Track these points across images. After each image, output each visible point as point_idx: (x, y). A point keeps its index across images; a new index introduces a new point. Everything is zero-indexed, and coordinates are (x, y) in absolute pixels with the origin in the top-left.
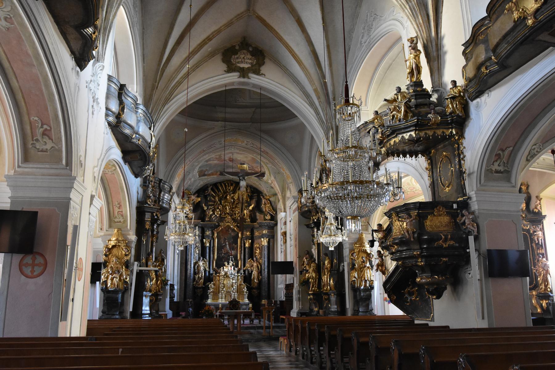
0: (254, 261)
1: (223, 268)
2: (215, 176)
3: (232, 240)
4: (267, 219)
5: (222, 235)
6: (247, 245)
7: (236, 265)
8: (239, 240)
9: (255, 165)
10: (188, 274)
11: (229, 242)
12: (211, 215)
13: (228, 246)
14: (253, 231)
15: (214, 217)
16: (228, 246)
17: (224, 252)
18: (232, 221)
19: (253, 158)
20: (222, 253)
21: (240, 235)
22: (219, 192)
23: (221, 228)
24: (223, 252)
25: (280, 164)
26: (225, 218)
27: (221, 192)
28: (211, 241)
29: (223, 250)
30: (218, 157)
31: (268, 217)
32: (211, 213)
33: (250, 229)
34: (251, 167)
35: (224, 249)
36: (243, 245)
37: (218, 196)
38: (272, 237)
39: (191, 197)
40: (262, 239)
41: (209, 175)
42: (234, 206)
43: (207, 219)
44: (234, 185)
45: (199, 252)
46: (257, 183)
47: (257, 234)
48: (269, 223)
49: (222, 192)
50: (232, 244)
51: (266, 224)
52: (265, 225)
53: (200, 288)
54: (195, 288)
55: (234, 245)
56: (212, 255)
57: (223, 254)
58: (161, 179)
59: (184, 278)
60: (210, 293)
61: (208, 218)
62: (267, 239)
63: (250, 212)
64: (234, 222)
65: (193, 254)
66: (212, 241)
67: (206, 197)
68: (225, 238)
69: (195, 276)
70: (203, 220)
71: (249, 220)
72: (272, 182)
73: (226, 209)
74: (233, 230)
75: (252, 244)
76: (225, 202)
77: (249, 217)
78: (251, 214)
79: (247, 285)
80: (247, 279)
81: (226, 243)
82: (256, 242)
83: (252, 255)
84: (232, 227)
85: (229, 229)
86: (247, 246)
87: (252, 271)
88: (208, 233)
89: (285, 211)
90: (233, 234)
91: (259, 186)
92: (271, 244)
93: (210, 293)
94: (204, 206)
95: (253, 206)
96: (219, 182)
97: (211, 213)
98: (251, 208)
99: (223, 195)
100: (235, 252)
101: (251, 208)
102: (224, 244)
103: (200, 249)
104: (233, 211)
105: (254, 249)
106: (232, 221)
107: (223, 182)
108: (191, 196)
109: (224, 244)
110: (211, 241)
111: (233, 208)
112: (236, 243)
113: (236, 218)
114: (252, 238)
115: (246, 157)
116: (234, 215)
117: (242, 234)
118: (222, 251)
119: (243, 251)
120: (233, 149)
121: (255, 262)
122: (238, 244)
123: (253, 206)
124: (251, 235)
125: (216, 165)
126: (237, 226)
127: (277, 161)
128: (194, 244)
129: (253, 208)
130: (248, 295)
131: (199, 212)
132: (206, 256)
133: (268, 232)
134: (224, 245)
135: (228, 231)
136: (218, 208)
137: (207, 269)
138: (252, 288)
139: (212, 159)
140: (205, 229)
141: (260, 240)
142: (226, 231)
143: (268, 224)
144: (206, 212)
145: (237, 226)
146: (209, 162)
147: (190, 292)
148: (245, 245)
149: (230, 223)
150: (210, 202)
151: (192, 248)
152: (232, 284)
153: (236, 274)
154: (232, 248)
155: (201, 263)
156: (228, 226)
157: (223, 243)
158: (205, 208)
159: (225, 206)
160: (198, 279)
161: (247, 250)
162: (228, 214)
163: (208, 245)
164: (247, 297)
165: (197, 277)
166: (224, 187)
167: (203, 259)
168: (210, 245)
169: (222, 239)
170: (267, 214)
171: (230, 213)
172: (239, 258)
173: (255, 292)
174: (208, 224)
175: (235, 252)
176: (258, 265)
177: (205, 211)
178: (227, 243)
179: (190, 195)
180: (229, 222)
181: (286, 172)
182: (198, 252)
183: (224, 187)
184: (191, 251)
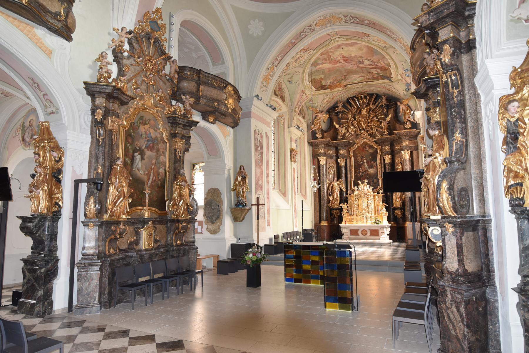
2: (340, 89)
4: (407, 129)
5: (359, 153)
9: (375, 58)
10: (322, 195)
11: (366, 160)
12: (345, 134)
13: (365, 164)
14: (394, 145)
15: (348, 136)
16: (365, 164)
17: (363, 170)
18: (369, 137)
19: (368, 46)
20: (360, 172)
21: (379, 152)
22: (351, 107)
23: (357, 146)
24: (361, 171)
25: (394, 34)
26: (360, 134)
27: (354, 107)
28: (346, 160)
29: (361, 169)
30: (325, 57)
31: (408, 126)
32: (344, 131)
33: (389, 143)
34: (372, 63)
35: (362, 168)
36: (382, 161)
37: (352, 112)
38: (414, 150)
39: (318, 115)
40: (402, 152)
41: (331, 87)
42: (369, 120)
43: (339, 138)
44: (368, 98)
45: (334, 172)
46: (391, 88)
47: (397, 147)
48: (410, 132)
49: (356, 107)
50: (371, 162)
51: (405, 134)
52: (404, 136)
53: (336, 209)
54: (330, 210)
55: (373, 162)
56: (349, 176)
57: (361, 173)
58: (199, 69)
59: (318, 199)
61: (341, 136)
62: (409, 151)
64: (370, 137)
65: (325, 175)
66: (348, 161)
67: (337, 114)
68: (362, 156)
69: (330, 197)
70: (335, 138)
71: (386, 133)
72: (402, 77)
73: (361, 124)
74: (371, 147)
75: (393, 159)
76: (359, 117)
77: (387, 129)
78: (388, 126)
79: (385, 206)
82: (397, 156)
84: (368, 143)
85: (366, 145)
88: (341, 152)
90: (371, 151)
91: (394, 90)
92: (415, 157)
94: (335, 125)
95: (390, 116)
96: (351, 98)
97: (344, 131)
98: (388, 119)
99: (356, 111)
100: (374, 170)
101: (388, 119)
102: (361, 163)
103: (335, 169)
104: (368, 126)
105: (396, 165)
106: (369, 137)
107: (355, 96)
108: (318, 114)
109: (361, 163)
110: (346, 160)
111: (369, 123)
113: (373, 133)
114: (393, 153)
115: (360, 49)
117: (381, 150)
119: (383, 169)
120: (337, 39)
122: (377, 161)
123: (390, 116)
124: (390, 149)
125: (329, 70)
126: (374, 141)
127: (388, 32)
129: (391, 119)
131: (331, 132)
132: (342, 176)
133: (409, 143)
134: (362, 164)
135: (365, 148)
136: (353, 125)
137: (344, 190)
138: (395, 209)
139: (319, 62)
140: (339, 148)
142: (363, 148)
146: (319, 67)
147: (324, 215)
149: (367, 139)
150: (342, 119)
151: (323, 168)
153: (372, 193)
154: (370, 167)
155: (335, 184)
156: (365, 142)
157: (360, 161)
158: (337, 126)
159: (360, 121)
160: (333, 200)
161: (387, 167)
162: (364, 129)
163: (343, 164)
165: (331, 198)
166: (357, 101)
167: (338, 180)
168: (346, 164)
170: (407, 122)
171: (366, 128)
172: (379, 177)
173: (398, 213)
174: (341, 142)
175: (374, 170)
177: (336, 130)
178: (365, 161)
179: (317, 113)
180: (365, 138)
181: (404, 44)
182: (333, 173)
183: (357, 101)
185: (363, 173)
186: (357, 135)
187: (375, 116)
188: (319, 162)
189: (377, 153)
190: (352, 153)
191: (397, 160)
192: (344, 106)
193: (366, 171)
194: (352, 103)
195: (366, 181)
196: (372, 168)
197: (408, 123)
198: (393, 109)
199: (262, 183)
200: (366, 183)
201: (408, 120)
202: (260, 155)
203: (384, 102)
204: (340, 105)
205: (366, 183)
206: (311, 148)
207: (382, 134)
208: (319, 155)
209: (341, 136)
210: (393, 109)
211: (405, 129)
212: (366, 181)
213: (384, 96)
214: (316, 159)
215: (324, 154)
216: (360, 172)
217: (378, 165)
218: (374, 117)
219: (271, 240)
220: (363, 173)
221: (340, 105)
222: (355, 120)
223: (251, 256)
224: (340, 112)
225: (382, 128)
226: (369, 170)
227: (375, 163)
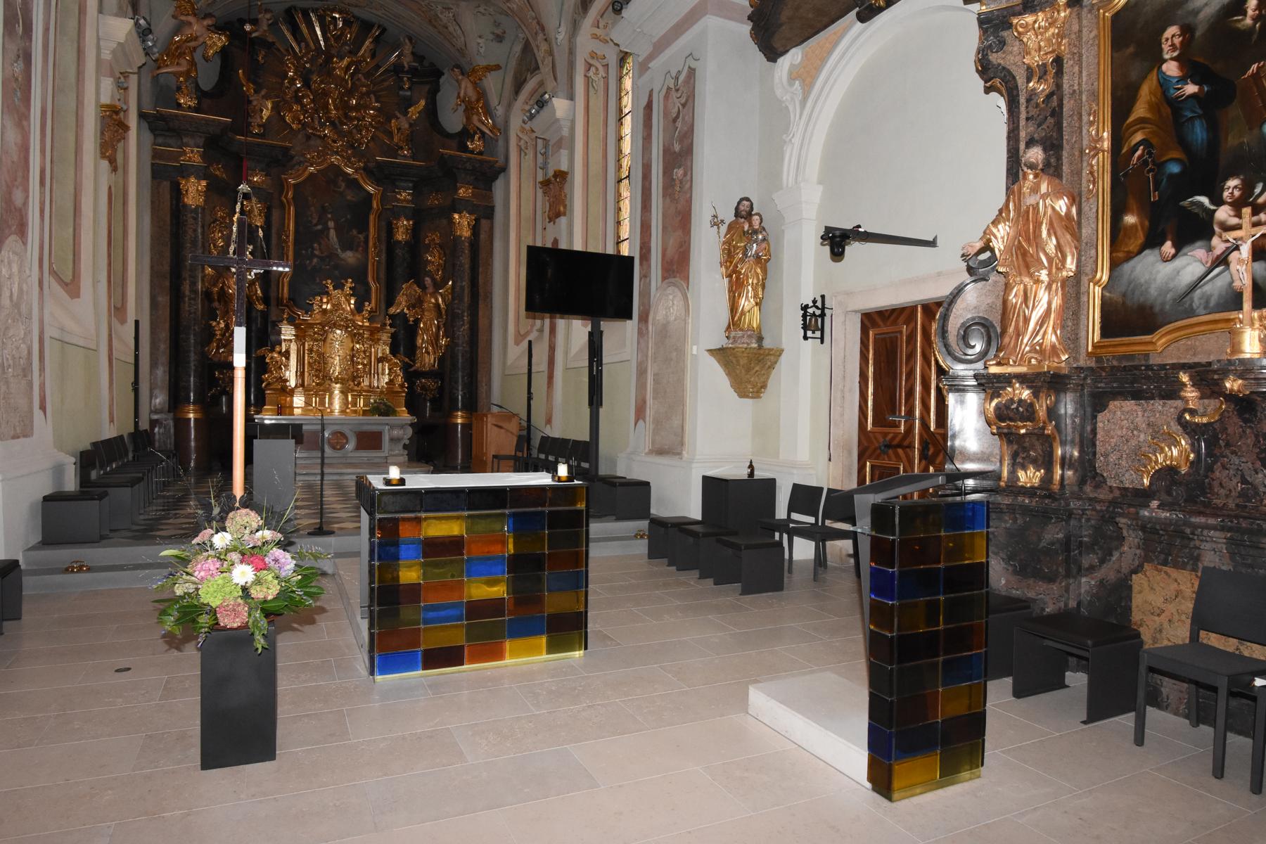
0: (424, 288)
1: (321, 300)
3: (349, 216)
6: (400, 236)
7: (362, 297)
8: (372, 217)
11: (336, 223)
13: (332, 233)
16: (332, 233)
20: (314, 256)
22: (299, 44)
24: (317, 253)
27: (307, 45)
35: (320, 244)
36: (384, 235)
39: (190, 24)
40: (456, 216)
46: (445, 17)
51: (468, 166)
55: (355, 232)
57: (315, 260)
60: (269, 384)
61: (259, 126)
63: (411, 125)
68: (323, 207)
73: (325, 107)
74: (353, 184)
75: (415, 232)
80: (404, 342)
81: (325, 224)
83: (415, 272)
86: (400, 238)
87: (417, 321)
89: (571, 97)
90: (350, 196)
92: (483, 236)
93: (269, 384)
98: (414, 112)
101: (414, 112)
102: (319, 227)
109: (319, 227)
112: (364, 228)
116: (354, 131)
117: (383, 199)
118: (313, 249)
121: (431, 290)
122: (366, 229)
126: (365, 169)
128: (203, 209)
130: (407, 393)
134: (322, 231)
136: (298, 100)
141: (445, 222)
143: (477, 165)
144: (250, 102)
145: (365, 169)
148: (390, 231)
151: (195, 219)
152: (353, 356)
154: (348, 245)
157: (315, 221)
158: (248, 88)
159: (326, 94)
161: (399, 252)
164: (403, 401)
169: (313, 208)
176: (437, 300)
178: (331, 224)
180: (337, 153)
184: (195, 231)
185: (322, 259)
186: (308, 137)
187: (374, 93)
188: (177, 193)
189: (371, 207)
190: (290, 195)
191: (432, 237)
192: (274, 26)
193: (332, 255)
194: (303, 27)
195: (349, 284)
196: (351, 249)
197: (476, 137)
198: (427, 88)
199: (25, 203)
200: (347, 290)
201: (478, 128)
202: (21, 62)
203: (407, 61)
204: (265, 19)
205: (347, 290)
206: (148, 137)
207: (393, 151)
208: (185, 171)
209: (259, 126)
210: (427, 88)
211: (465, 149)
212: (349, 284)
213: (410, 39)
214: (166, 185)
215: (203, 174)
216: (314, 256)
217: (371, 244)
218: (368, 94)
219: (58, 470)
220: (322, 259)
221: (265, 19)
222: (307, 84)
223: (243, 574)
224: (262, 42)
225: (390, 134)
226: (343, 255)
227: (361, 237)
